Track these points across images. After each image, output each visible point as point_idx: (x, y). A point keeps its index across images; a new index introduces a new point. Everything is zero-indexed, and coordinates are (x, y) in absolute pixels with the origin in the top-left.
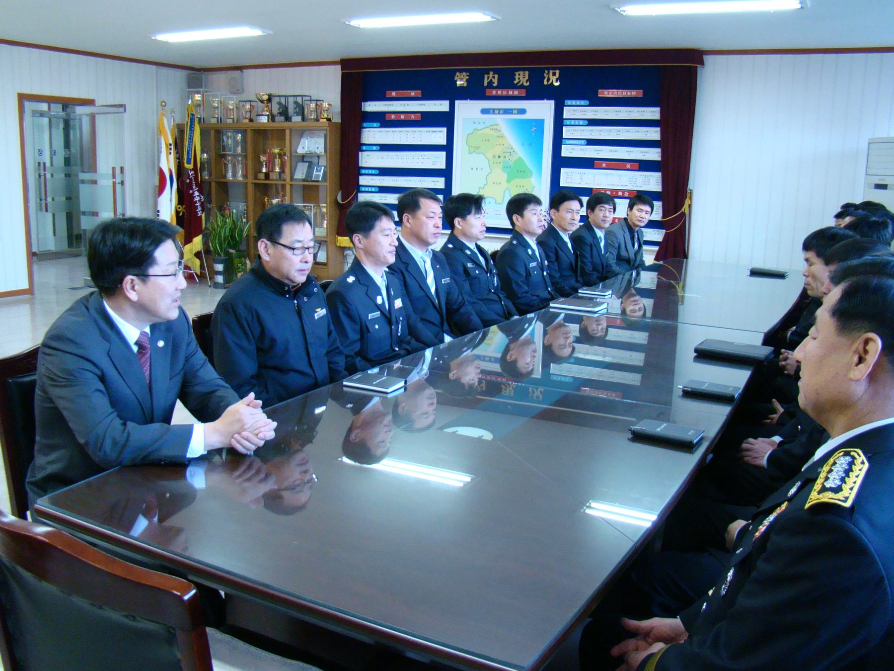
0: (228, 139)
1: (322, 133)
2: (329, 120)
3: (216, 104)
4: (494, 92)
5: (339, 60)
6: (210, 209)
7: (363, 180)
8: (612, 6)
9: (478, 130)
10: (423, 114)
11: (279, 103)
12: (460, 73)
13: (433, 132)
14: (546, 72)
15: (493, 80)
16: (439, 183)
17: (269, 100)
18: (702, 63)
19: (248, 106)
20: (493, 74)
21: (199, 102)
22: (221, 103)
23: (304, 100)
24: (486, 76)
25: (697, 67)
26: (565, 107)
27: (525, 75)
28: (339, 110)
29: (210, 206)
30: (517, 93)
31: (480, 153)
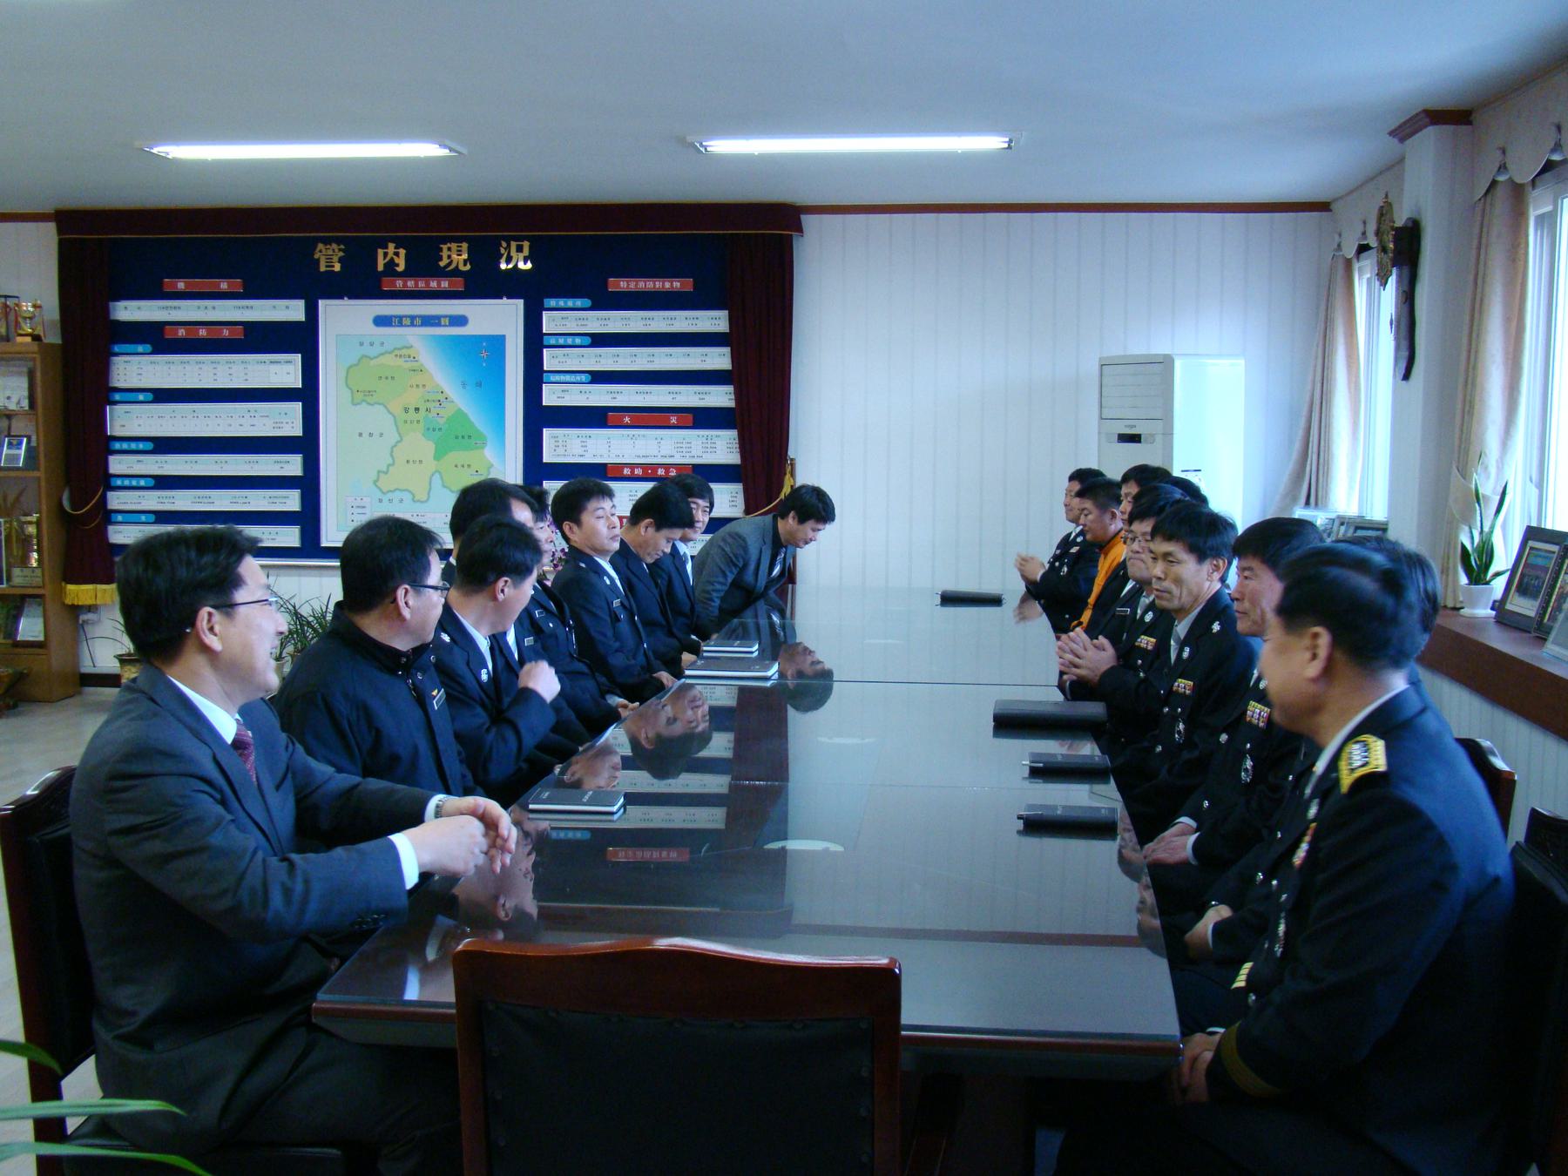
2: (36, 338)
4: (399, 284)
7: (117, 465)
8: (689, 139)
9: (372, 359)
10: (250, 327)
12: (325, 244)
14: (504, 244)
15: (396, 260)
16: (292, 465)
18: (800, 229)
20: (395, 248)
24: (380, 252)
25: (791, 235)
27: (460, 251)
31: (376, 403)
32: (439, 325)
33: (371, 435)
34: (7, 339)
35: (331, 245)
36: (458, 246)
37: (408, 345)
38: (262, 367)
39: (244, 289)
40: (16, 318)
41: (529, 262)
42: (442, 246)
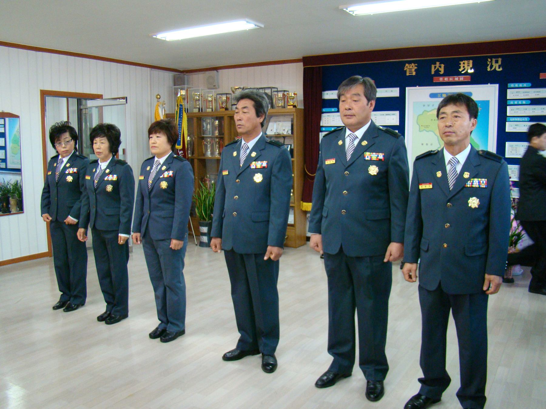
0: (207, 125)
1: (289, 119)
2: (295, 106)
3: (198, 97)
4: (441, 79)
5: (302, 58)
13: (386, 115)
14: (489, 60)
15: (440, 69)
19: (224, 98)
20: (440, 64)
21: (184, 97)
22: (202, 97)
23: (272, 91)
24: (433, 66)
26: (508, 90)
27: (469, 64)
28: (302, 99)
30: (462, 79)
31: (429, 131)
33: (427, 144)
34: (284, 107)
35: (411, 64)
36: (468, 62)
38: (383, 117)
40: (288, 99)
41: (501, 68)
42: (460, 62)
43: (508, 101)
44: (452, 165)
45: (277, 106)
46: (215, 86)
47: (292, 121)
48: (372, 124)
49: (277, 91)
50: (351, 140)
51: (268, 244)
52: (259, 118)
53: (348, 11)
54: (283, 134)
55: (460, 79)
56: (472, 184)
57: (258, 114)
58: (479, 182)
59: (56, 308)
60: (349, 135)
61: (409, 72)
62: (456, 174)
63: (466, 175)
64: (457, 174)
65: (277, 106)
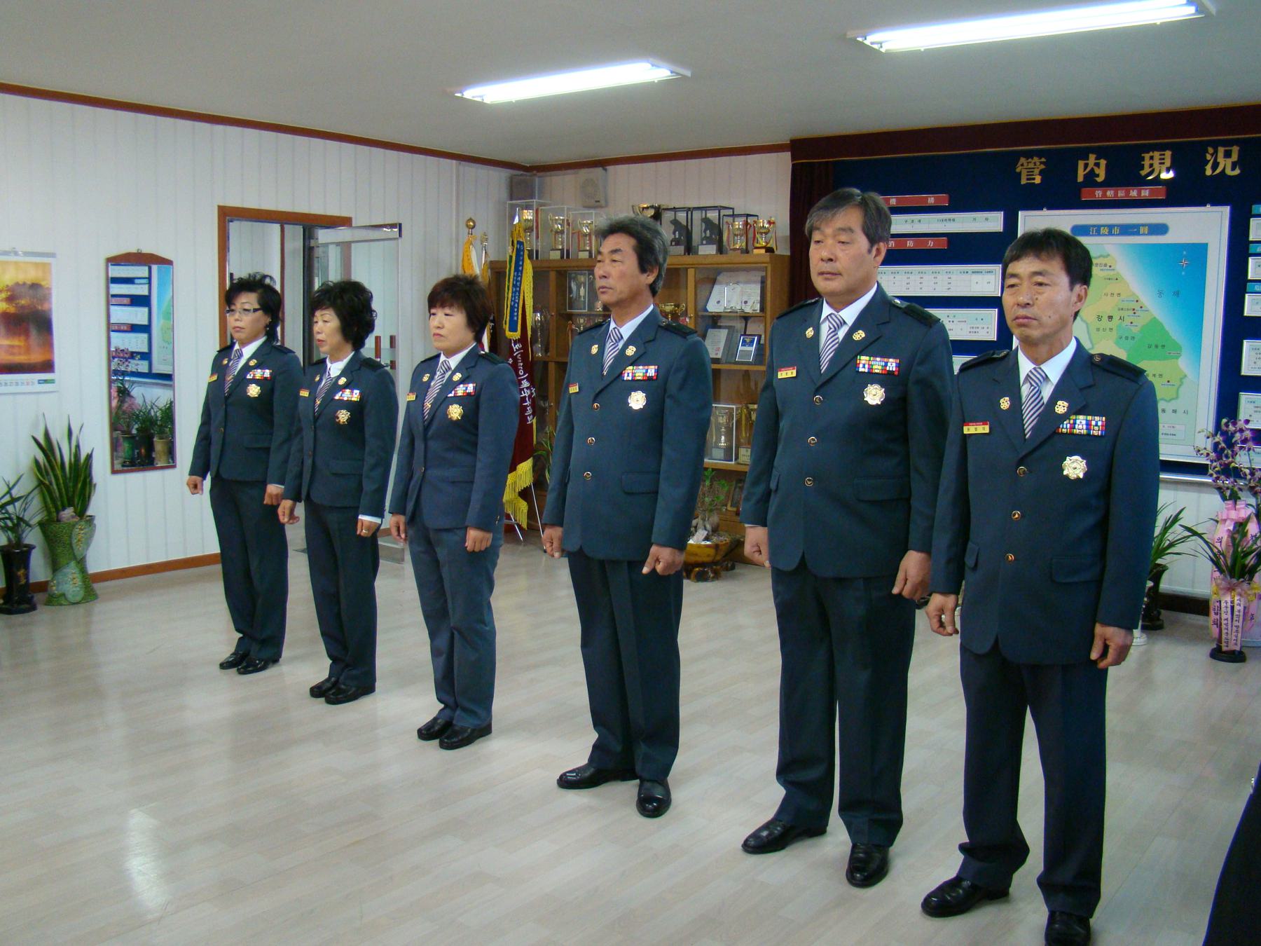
1: (757, 276)
2: (769, 250)
3: (560, 226)
4: (1099, 194)
6: (544, 410)
10: (952, 237)
11: (675, 222)
13: (973, 272)
14: (1211, 150)
15: (1097, 171)
17: (657, 216)
20: (1096, 159)
21: (530, 224)
22: (568, 224)
24: (1081, 164)
27: (1163, 159)
28: (788, 233)
29: (544, 404)
32: (1138, 233)
34: (747, 251)
35: (1032, 158)
36: (1161, 155)
37: (1105, 254)
39: (950, 203)
42: (1143, 155)
43: (1251, 245)
44: (1032, 385)
45: (731, 250)
46: (599, 201)
47: (763, 282)
48: (880, 291)
49: (733, 216)
50: (830, 328)
51: (653, 541)
52: (646, 275)
53: (867, 42)
54: (743, 311)
55: (1143, 194)
56: (1073, 427)
57: (644, 266)
58: (1088, 424)
59: (225, 666)
60: (829, 317)
61: (1028, 175)
62: (1041, 402)
63: (1061, 407)
64: (1043, 403)
65: (732, 247)
